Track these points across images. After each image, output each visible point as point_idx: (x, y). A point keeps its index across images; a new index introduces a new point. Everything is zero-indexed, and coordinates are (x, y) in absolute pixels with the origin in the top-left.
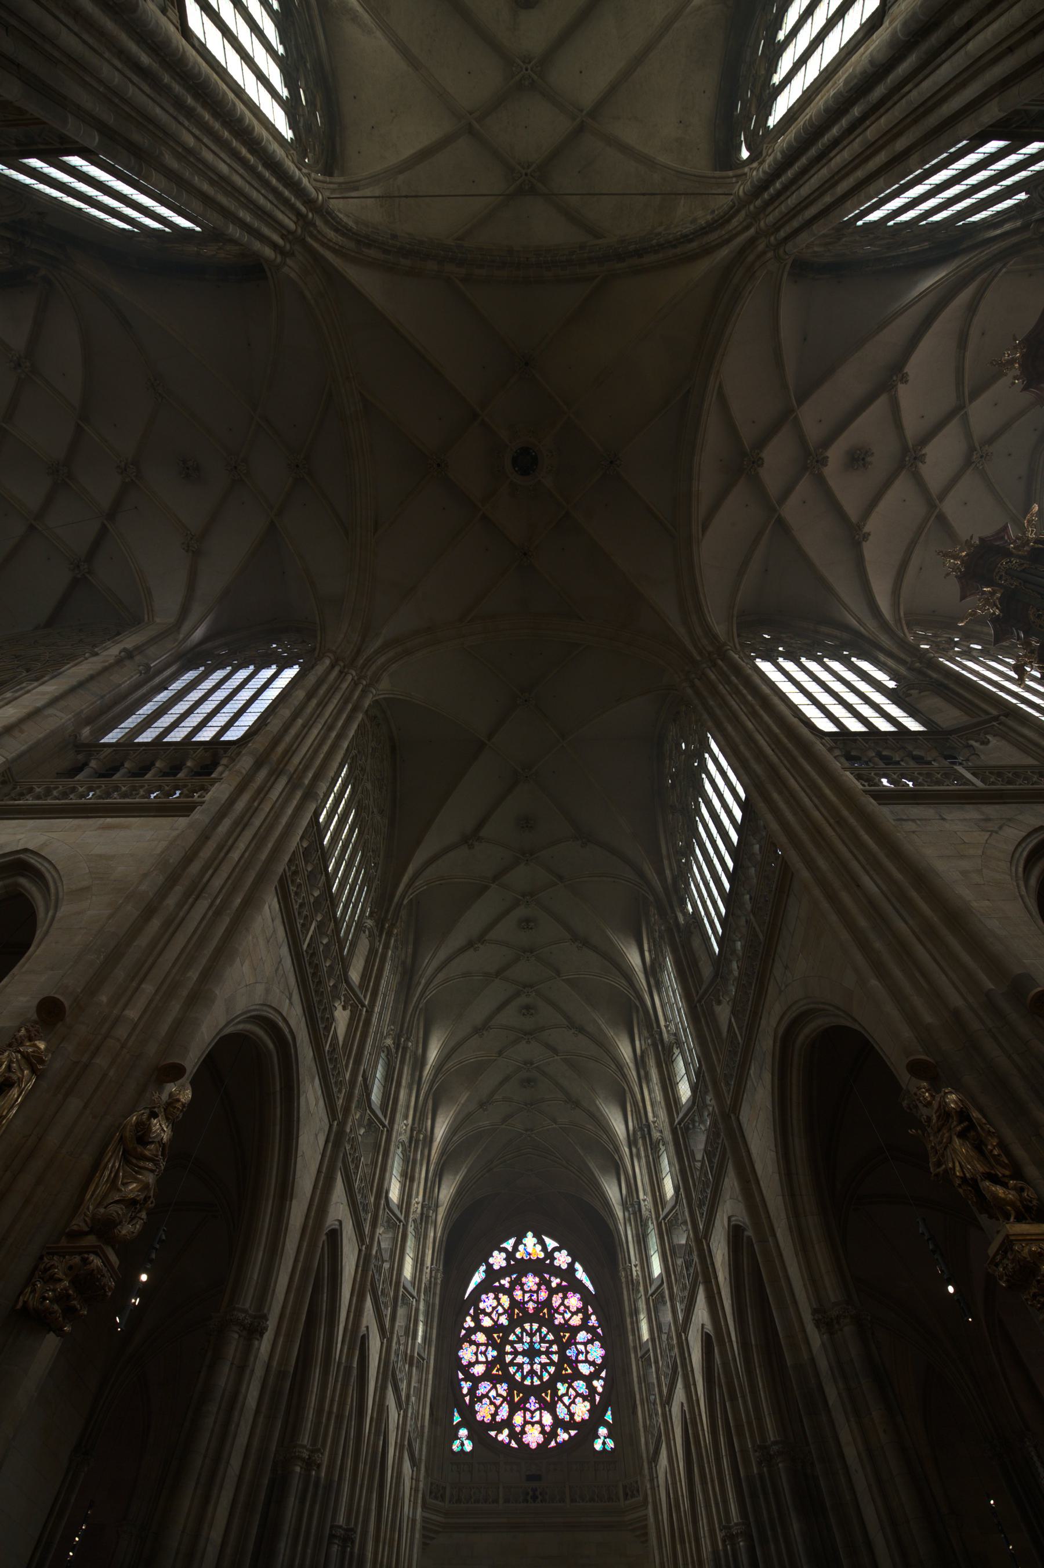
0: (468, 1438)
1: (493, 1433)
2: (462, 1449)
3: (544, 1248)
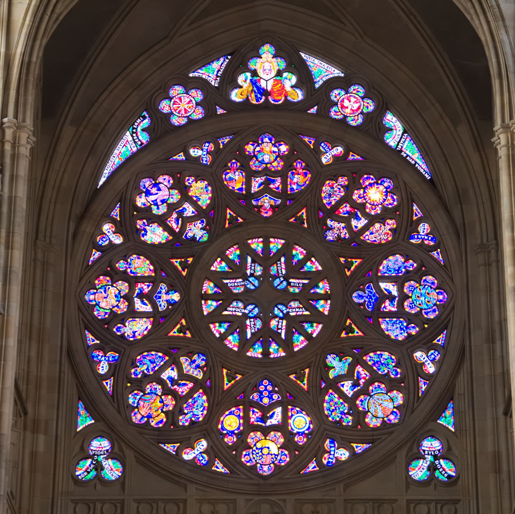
0: (111, 455)
1: (170, 448)
2: (99, 478)
3: (305, 78)
